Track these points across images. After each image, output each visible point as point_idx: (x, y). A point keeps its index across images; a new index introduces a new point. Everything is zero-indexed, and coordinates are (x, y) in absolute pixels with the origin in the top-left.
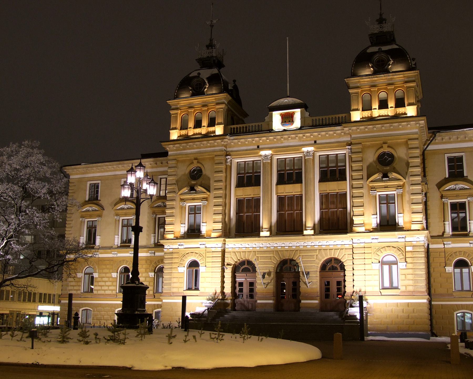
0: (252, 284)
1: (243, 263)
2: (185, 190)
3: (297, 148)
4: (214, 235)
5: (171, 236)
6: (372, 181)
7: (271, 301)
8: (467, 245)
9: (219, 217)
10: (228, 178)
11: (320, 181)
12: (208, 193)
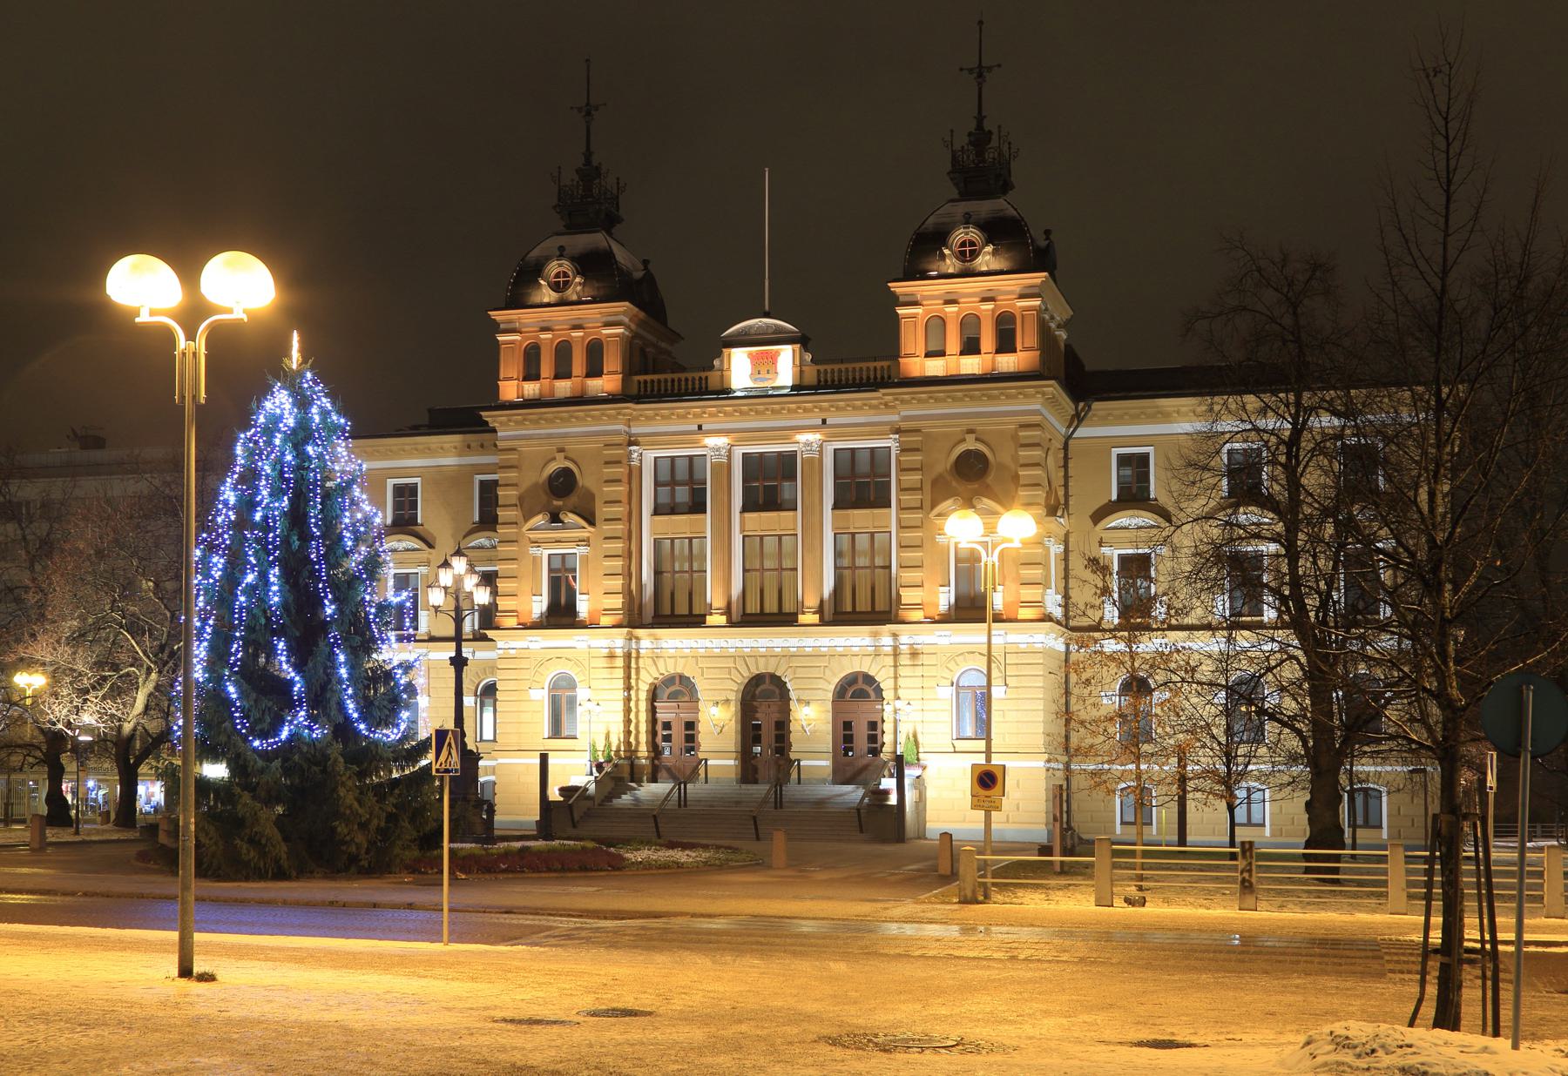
0: (690, 725)
1: (669, 680)
2: (539, 520)
3: (787, 432)
4: (605, 620)
5: (512, 622)
7: (732, 762)
9: (617, 583)
10: (634, 496)
11: (836, 507)
12: (591, 529)
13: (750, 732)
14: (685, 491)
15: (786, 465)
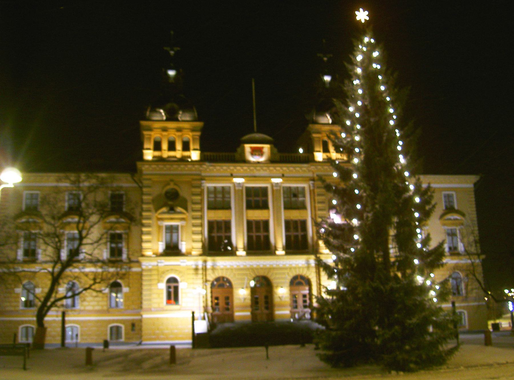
0: (227, 298)
1: (218, 279)
2: (164, 209)
12: (187, 214)
13: (255, 301)
14: (220, 201)
15: (264, 191)
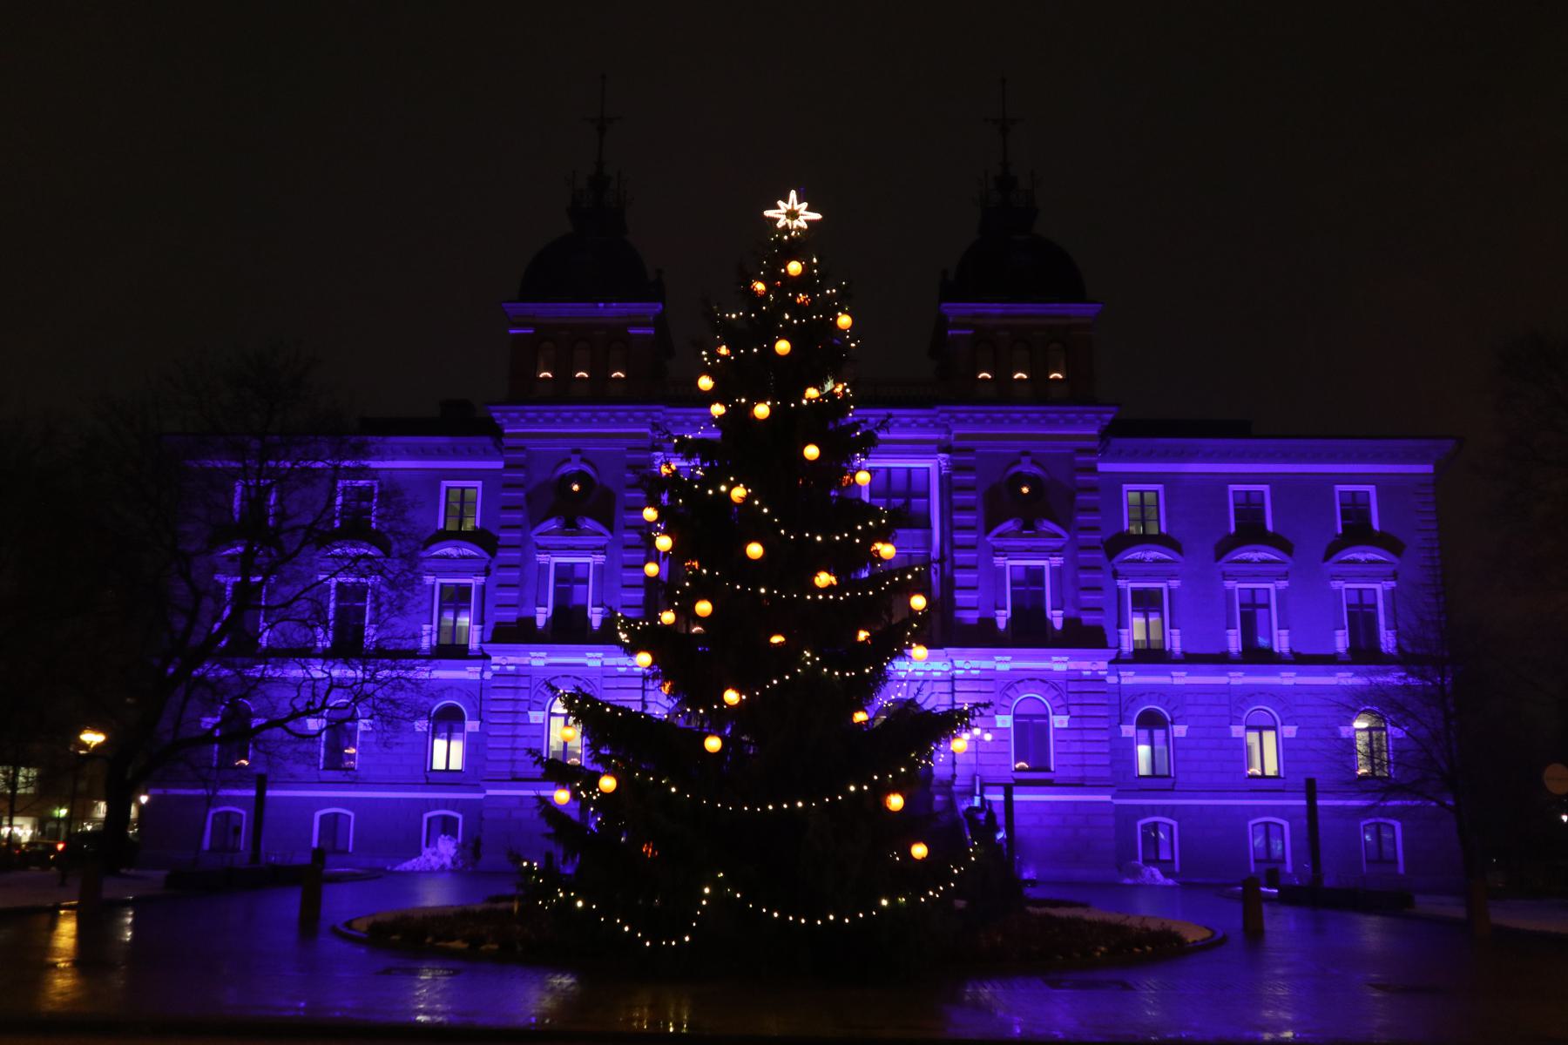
2: (553, 524)
6: (999, 535)
8: (1164, 680)
